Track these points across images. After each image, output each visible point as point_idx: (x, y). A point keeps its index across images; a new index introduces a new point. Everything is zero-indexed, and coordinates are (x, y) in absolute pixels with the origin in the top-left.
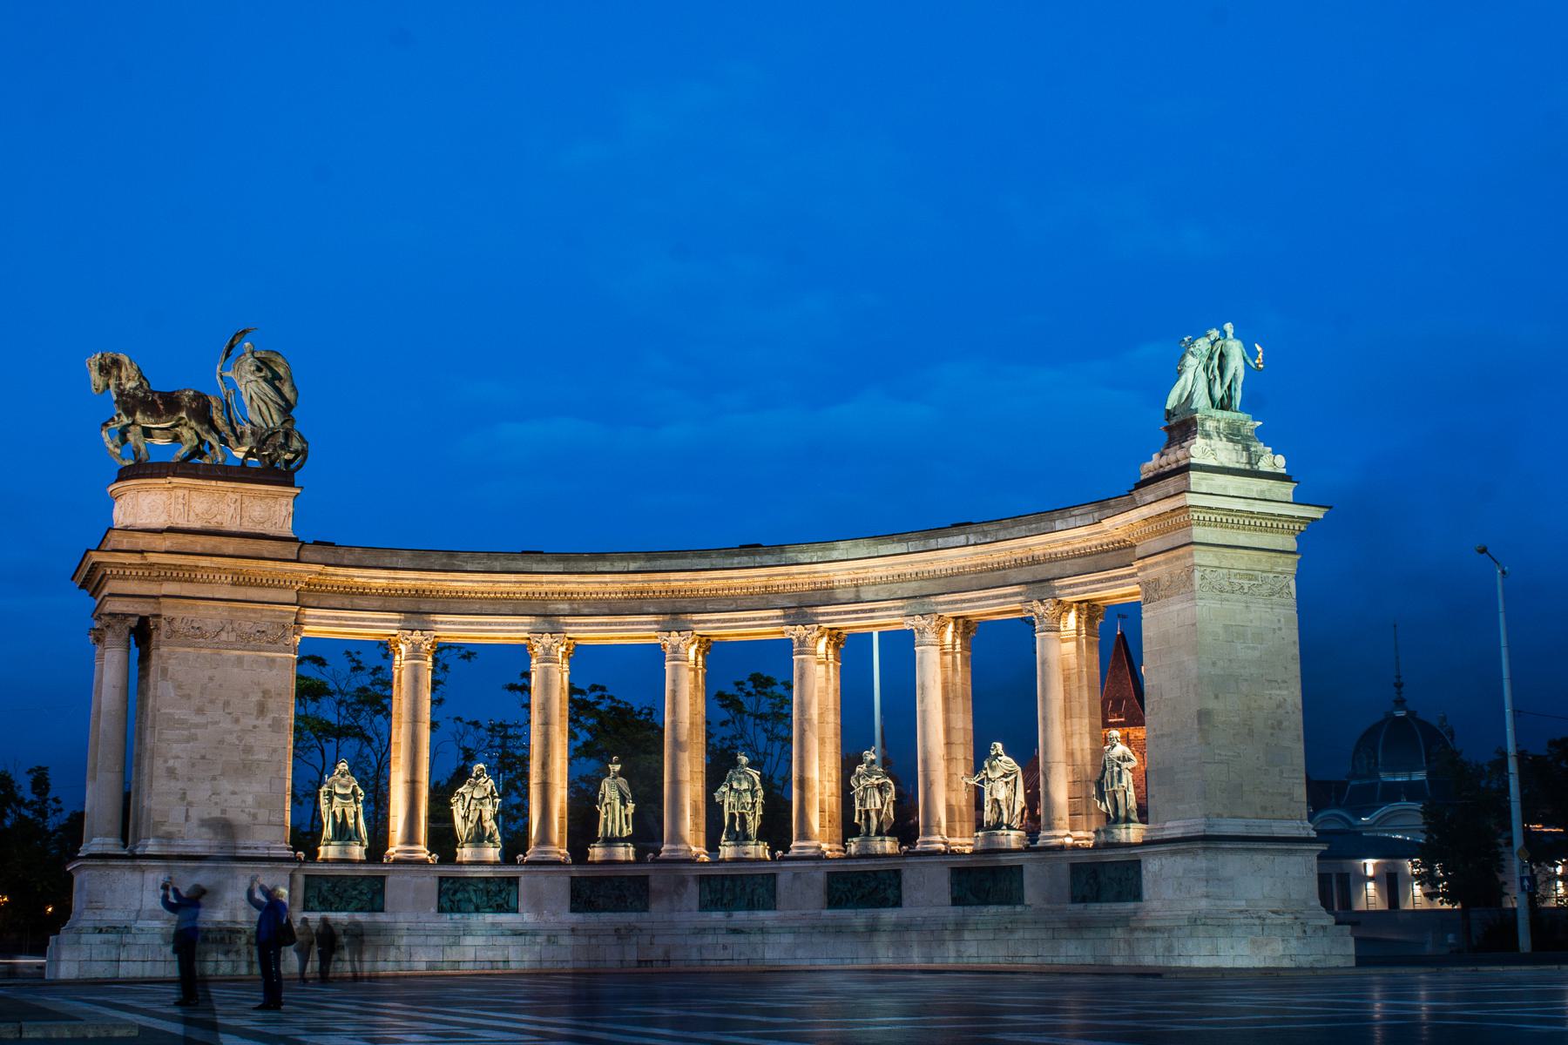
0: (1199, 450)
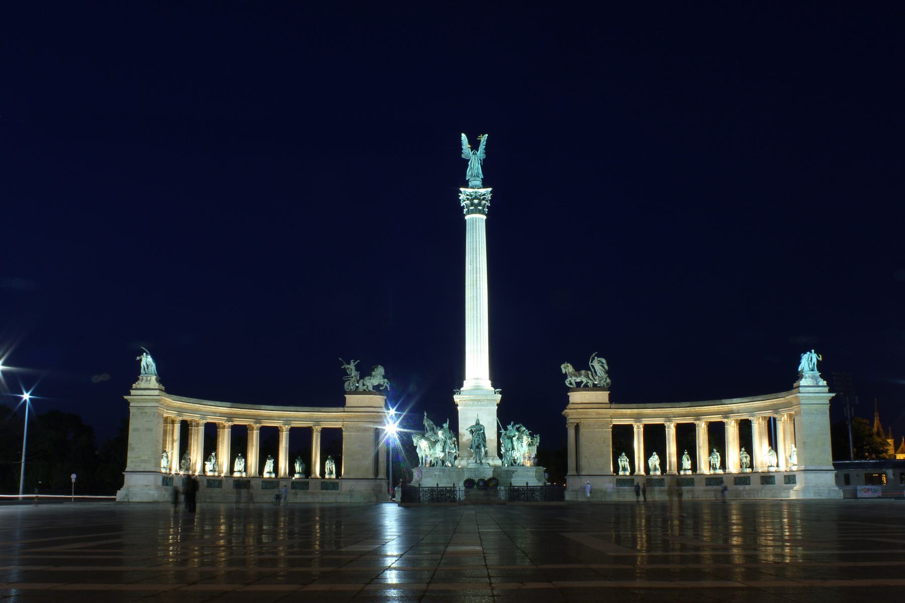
0: (803, 382)
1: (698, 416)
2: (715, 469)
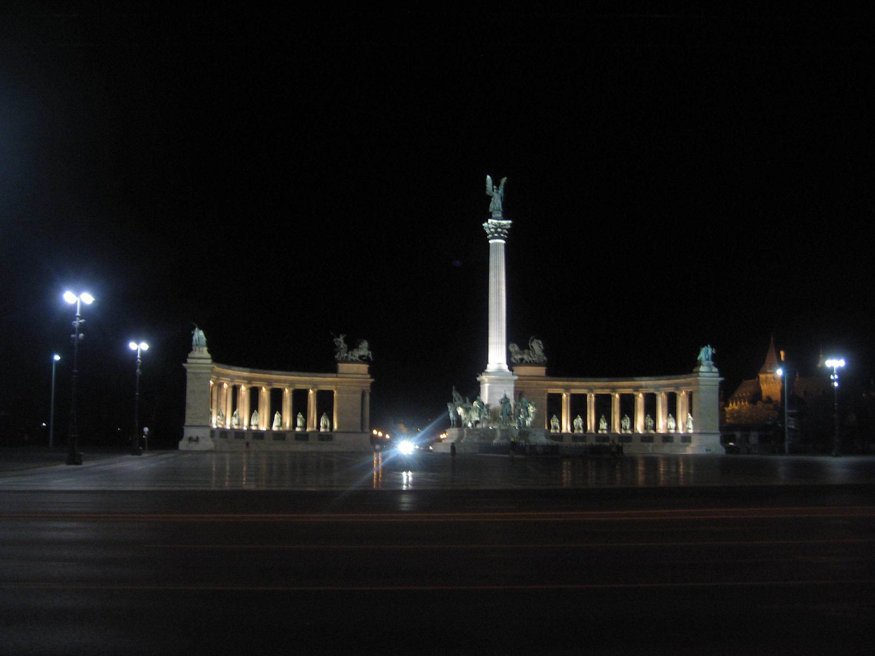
0: (702, 369)
1: (614, 389)
2: (625, 429)
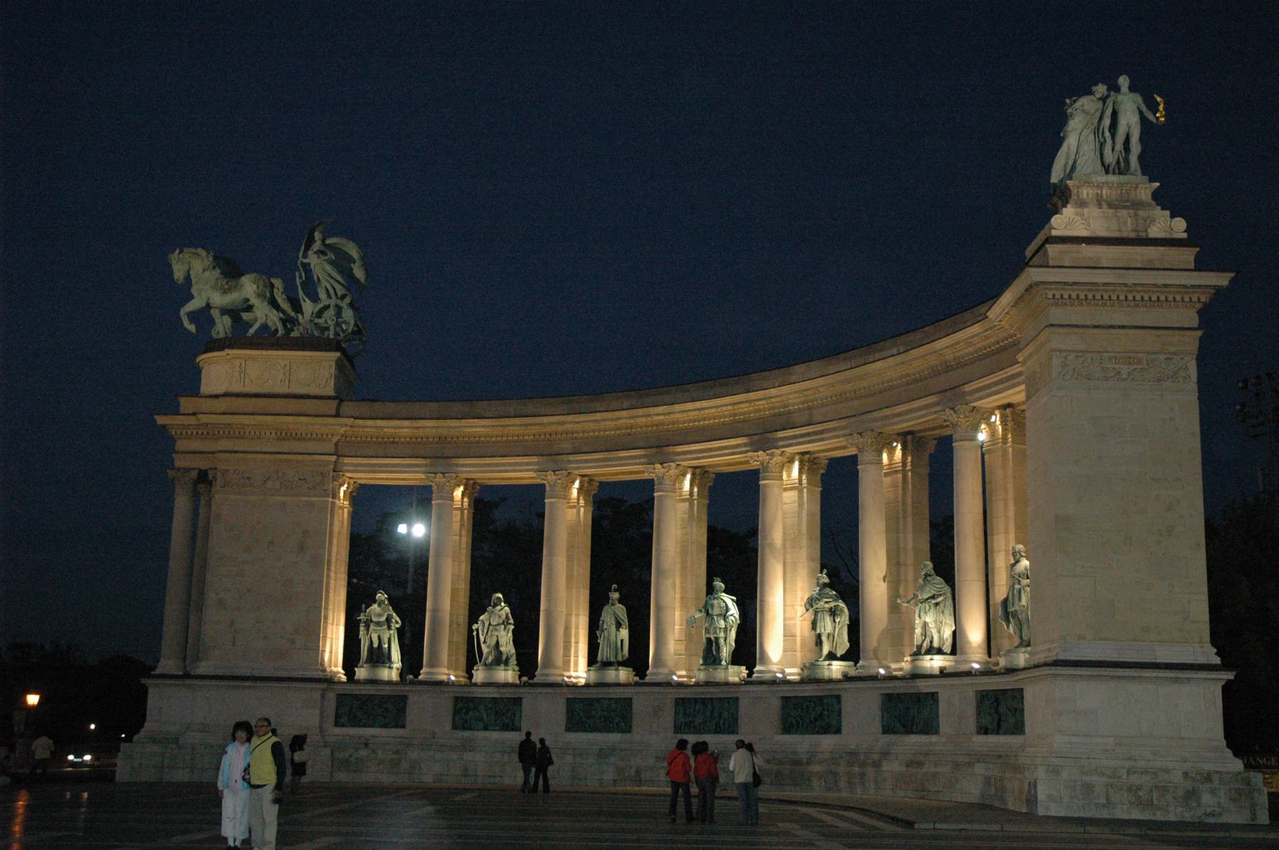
0: (1065, 222)
1: (660, 445)
